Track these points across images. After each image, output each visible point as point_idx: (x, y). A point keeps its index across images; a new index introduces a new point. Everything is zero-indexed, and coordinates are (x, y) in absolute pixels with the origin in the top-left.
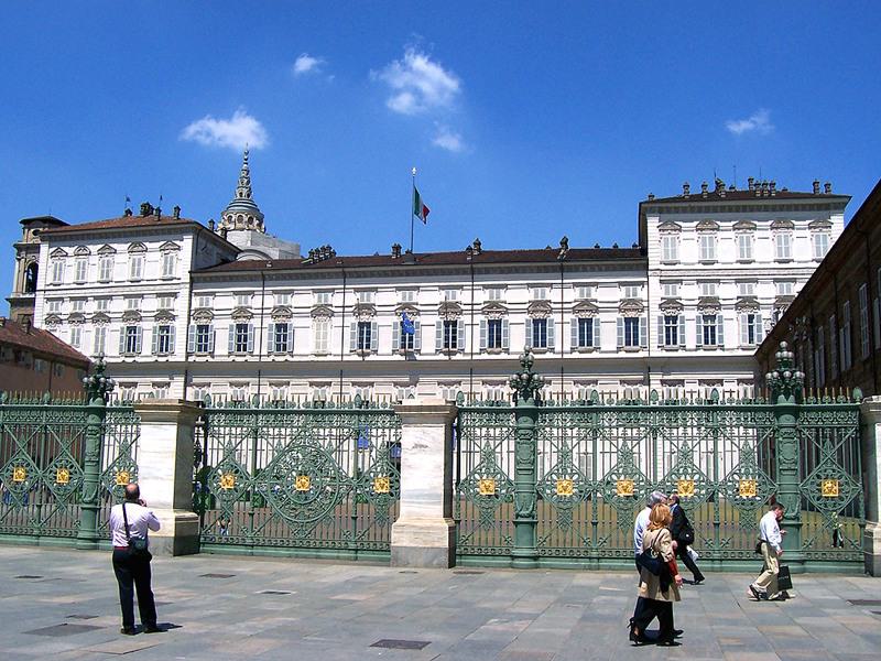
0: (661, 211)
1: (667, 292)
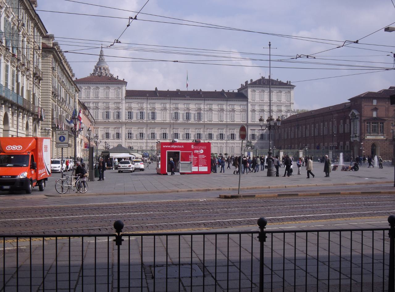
0: (252, 87)
1: (252, 107)
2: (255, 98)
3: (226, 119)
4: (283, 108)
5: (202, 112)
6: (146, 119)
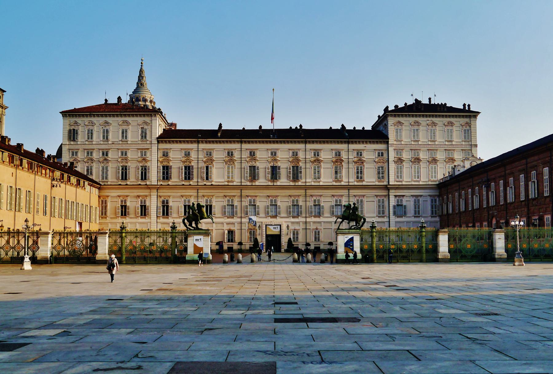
0: (395, 116)
1: (397, 155)
2: (401, 136)
3: (348, 177)
4: (458, 156)
5: (301, 164)
6: (195, 180)
